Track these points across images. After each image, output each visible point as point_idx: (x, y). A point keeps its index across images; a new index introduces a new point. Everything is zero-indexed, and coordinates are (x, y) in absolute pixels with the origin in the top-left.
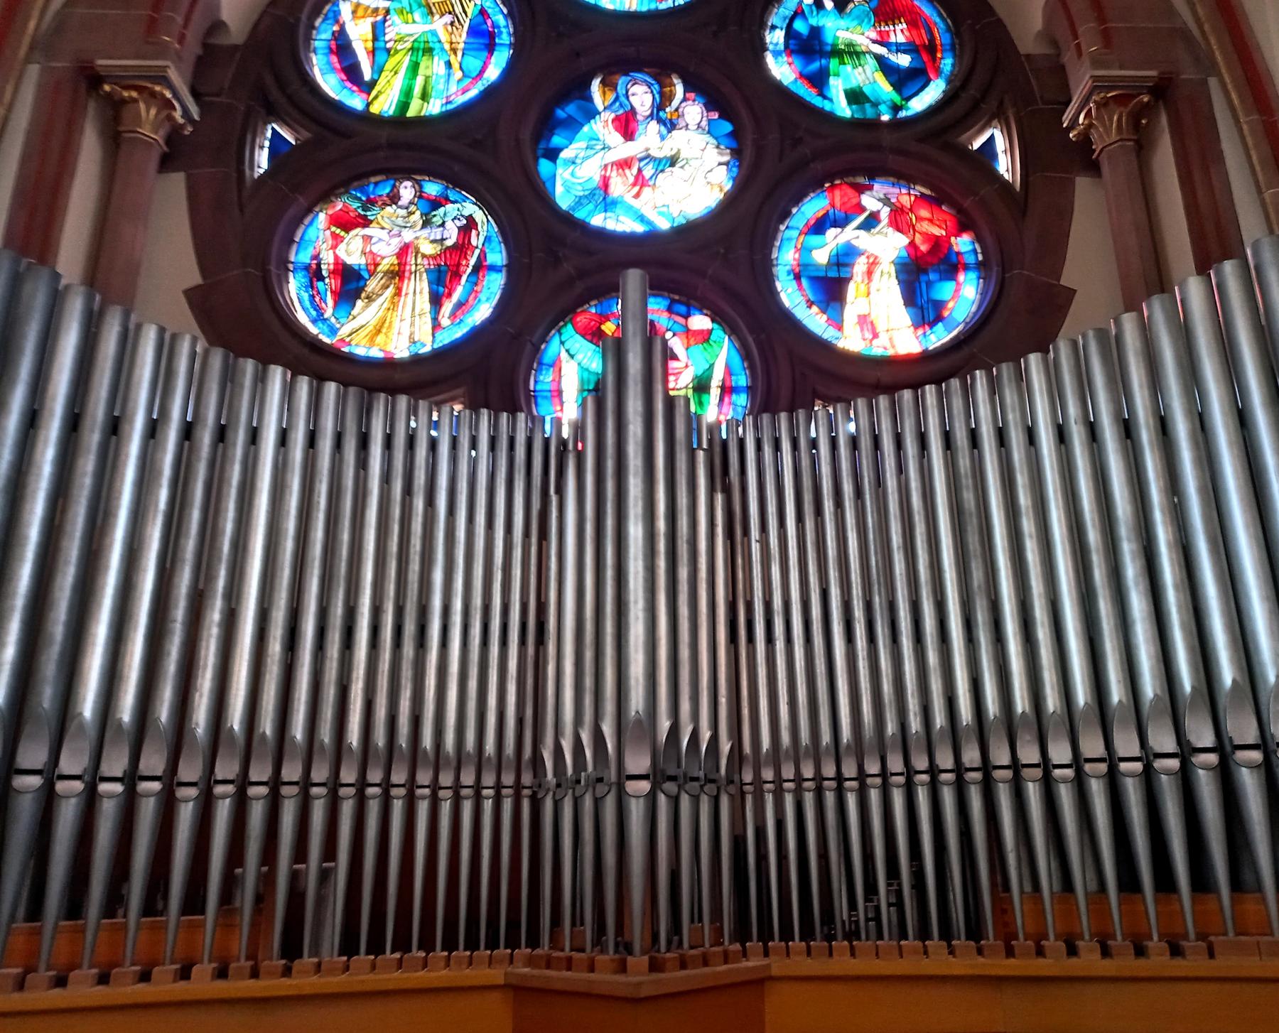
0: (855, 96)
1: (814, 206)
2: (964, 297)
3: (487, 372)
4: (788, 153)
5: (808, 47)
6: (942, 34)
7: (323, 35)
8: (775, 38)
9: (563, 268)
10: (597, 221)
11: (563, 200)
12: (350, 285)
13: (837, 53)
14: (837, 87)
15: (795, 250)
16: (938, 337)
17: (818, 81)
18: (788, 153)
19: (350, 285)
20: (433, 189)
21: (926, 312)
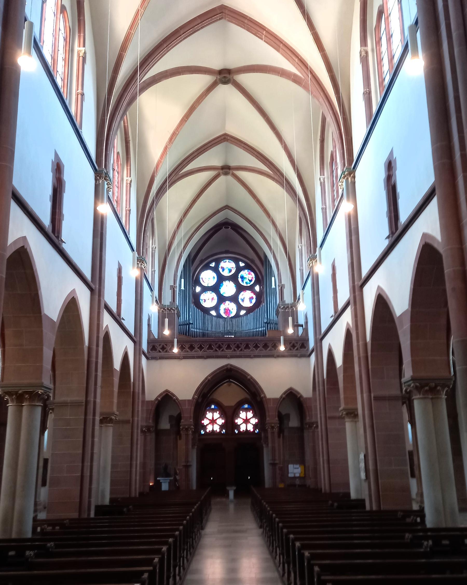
0: (246, 283)
1: (242, 293)
2: (254, 301)
3: (217, 308)
4: (240, 289)
5: (242, 278)
6: (254, 277)
7: (201, 277)
8: (239, 277)
9: (222, 299)
10: (224, 295)
11: (221, 293)
12: (205, 301)
13: (245, 278)
14: (245, 282)
15: (241, 296)
16: (251, 305)
17: (243, 281)
18: (240, 289)
19: (205, 301)
20: (211, 292)
21: (251, 302)
